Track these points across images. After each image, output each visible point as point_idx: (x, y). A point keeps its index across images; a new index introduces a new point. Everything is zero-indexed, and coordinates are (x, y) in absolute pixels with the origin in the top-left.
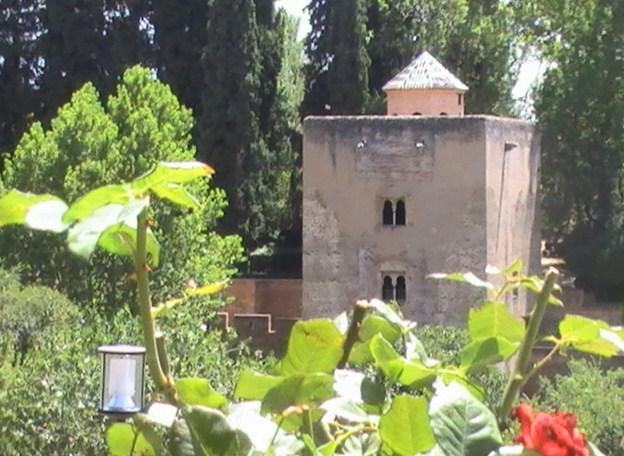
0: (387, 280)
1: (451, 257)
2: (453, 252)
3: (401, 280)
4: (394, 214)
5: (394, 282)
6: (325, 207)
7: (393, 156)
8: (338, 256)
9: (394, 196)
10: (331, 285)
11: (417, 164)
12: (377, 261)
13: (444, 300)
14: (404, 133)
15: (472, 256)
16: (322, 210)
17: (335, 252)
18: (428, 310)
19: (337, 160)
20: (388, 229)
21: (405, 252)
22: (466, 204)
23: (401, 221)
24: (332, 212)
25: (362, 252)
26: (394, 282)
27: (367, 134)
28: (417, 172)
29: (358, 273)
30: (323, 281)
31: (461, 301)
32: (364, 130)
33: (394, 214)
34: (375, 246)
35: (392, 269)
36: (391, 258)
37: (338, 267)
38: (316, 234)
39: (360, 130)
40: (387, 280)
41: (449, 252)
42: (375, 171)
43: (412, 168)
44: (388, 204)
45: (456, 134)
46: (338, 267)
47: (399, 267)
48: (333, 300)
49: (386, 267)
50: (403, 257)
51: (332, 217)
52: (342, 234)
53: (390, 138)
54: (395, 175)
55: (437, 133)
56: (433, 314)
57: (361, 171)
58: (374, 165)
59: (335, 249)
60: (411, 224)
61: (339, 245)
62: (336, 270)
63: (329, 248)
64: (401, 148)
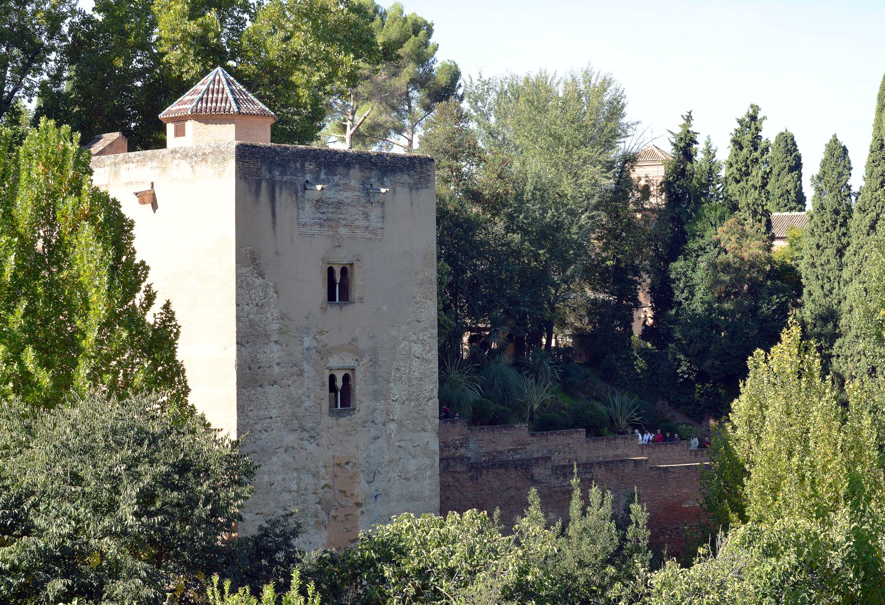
0: (332, 378)
1: (403, 344)
2: (405, 338)
3: (346, 378)
4: (338, 286)
5: (339, 384)
6: (262, 275)
7: (340, 203)
8: (278, 346)
9: (341, 258)
10: (272, 391)
11: (366, 216)
12: (324, 353)
13: (397, 405)
14: (352, 171)
15: (423, 343)
16: (259, 281)
17: (276, 342)
18: (379, 419)
19: (277, 210)
20: (333, 311)
21: (353, 339)
22: (416, 273)
23: (345, 297)
24: (271, 284)
25: (308, 342)
26: (339, 384)
27: (311, 172)
28: (367, 228)
29: (301, 373)
30: (261, 386)
31: (413, 404)
32: (307, 164)
33: (338, 286)
34: (321, 333)
35: (340, 364)
36: (340, 349)
37: (278, 364)
38: (251, 316)
39: (303, 165)
40: (332, 378)
41: (400, 338)
42: (321, 225)
43: (362, 223)
44: (331, 271)
45: (405, 178)
46: (278, 364)
47: (349, 362)
48: (274, 413)
49: (334, 362)
50: (352, 347)
51: (271, 291)
52: (283, 317)
53: (337, 178)
54: (343, 231)
55: (386, 176)
56: (384, 424)
57: (304, 225)
58: (319, 215)
59: (275, 338)
60: (361, 300)
61: (281, 332)
62: (276, 369)
63: (267, 336)
64: (349, 194)
